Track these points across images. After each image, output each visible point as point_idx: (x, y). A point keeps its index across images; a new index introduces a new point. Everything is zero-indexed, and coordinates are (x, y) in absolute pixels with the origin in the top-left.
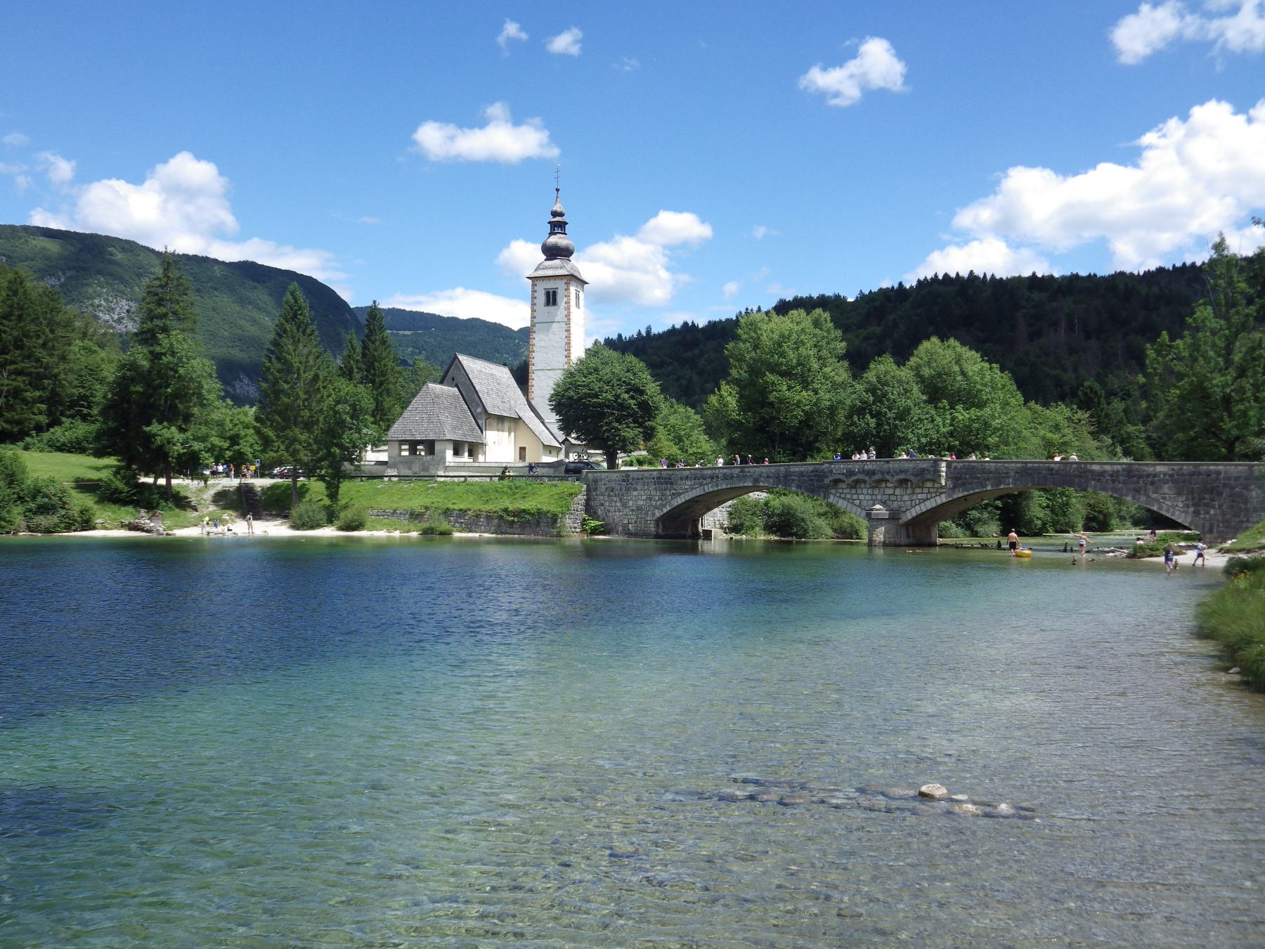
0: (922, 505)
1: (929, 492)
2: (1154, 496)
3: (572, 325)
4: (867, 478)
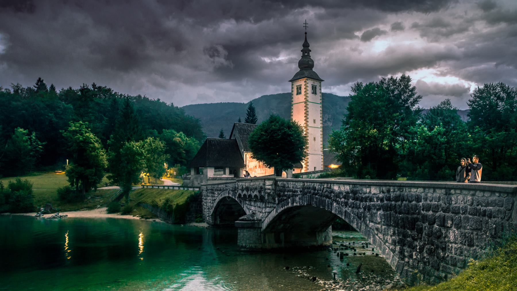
1: (270, 207)
2: (371, 224)
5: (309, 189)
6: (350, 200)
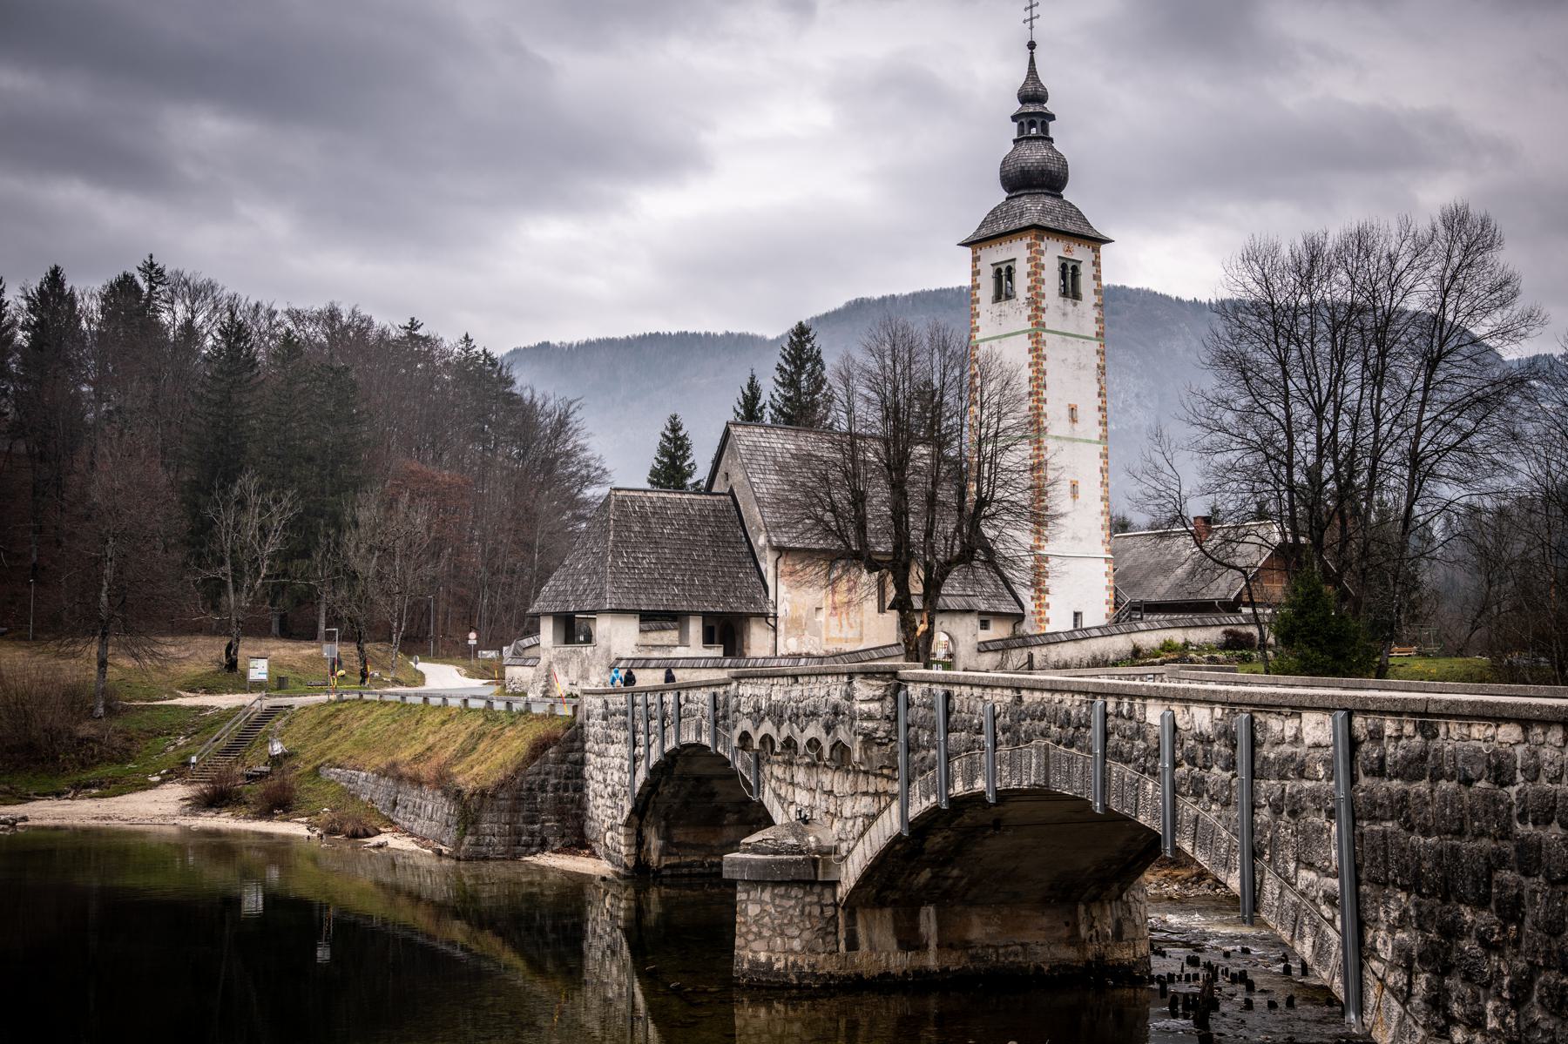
0: (866, 837)
1: (877, 794)
2: (1306, 876)
3: (1045, 336)
4: (774, 734)
5: (1041, 720)
6: (1216, 770)
